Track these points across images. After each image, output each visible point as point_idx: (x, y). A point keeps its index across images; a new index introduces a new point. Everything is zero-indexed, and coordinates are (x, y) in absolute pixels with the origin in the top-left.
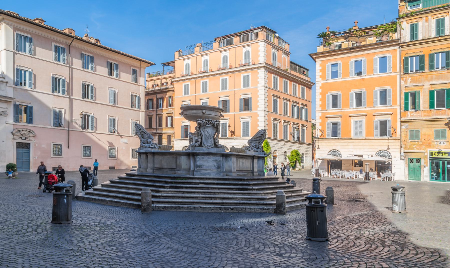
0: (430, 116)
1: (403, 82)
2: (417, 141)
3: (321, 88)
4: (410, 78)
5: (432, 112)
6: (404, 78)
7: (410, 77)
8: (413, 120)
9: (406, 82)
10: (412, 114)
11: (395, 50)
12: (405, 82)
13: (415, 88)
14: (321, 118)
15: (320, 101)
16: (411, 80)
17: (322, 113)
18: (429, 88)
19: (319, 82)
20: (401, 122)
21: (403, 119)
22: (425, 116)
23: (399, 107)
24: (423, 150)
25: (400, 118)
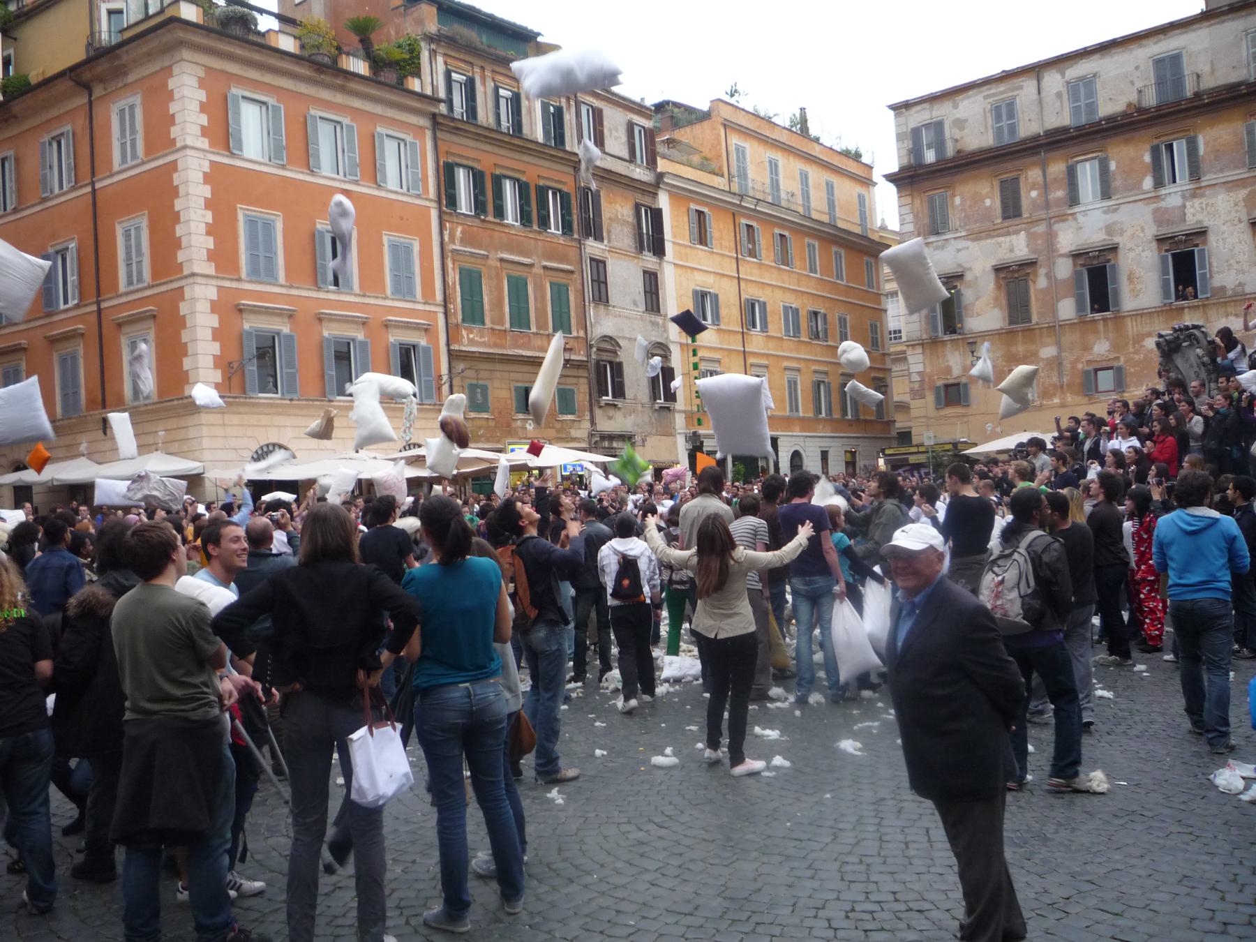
0: (503, 347)
1: (446, 238)
2: (485, 415)
3: (207, 178)
4: (459, 229)
5: (508, 338)
6: (448, 225)
7: (461, 224)
8: (477, 355)
9: (452, 236)
10: (471, 336)
11: (422, 128)
12: (450, 234)
13: (472, 260)
14: (215, 307)
15: (208, 233)
16: (462, 233)
17: (219, 287)
18: (496, 267)
19: (201, 155)
20: (452, 355)
21: (455, 347)
22: (496, 345)
23: (441, 310)
24: (498, 442)
25: (448, 345)
